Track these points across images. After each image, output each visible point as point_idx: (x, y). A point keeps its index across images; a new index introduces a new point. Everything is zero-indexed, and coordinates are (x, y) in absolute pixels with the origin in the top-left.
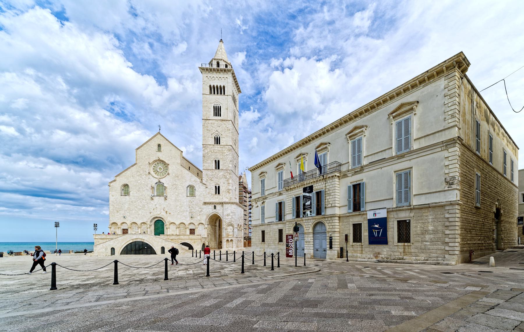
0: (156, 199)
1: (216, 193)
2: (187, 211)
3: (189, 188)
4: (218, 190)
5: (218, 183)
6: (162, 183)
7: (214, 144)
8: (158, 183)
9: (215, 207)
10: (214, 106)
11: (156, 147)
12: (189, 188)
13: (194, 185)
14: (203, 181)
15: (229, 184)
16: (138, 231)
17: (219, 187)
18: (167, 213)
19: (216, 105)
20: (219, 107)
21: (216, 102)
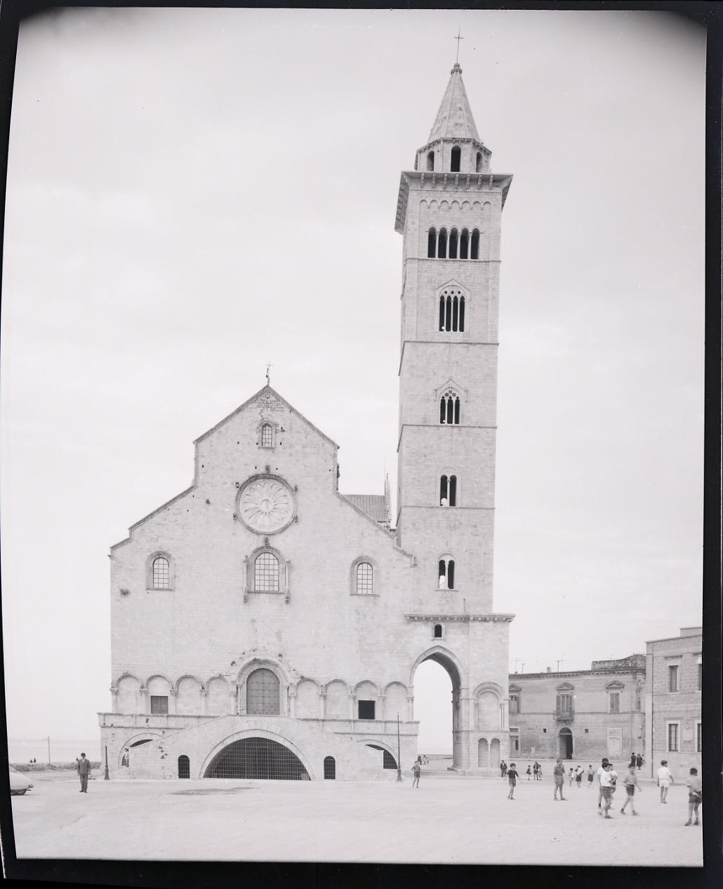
7: (439, 423)
9: (438, 632)
10: (442, 298)
12: (356, 566)
14: (402, 544)
19: (449, 293)
20: (459, 300)
21: (450, 284)
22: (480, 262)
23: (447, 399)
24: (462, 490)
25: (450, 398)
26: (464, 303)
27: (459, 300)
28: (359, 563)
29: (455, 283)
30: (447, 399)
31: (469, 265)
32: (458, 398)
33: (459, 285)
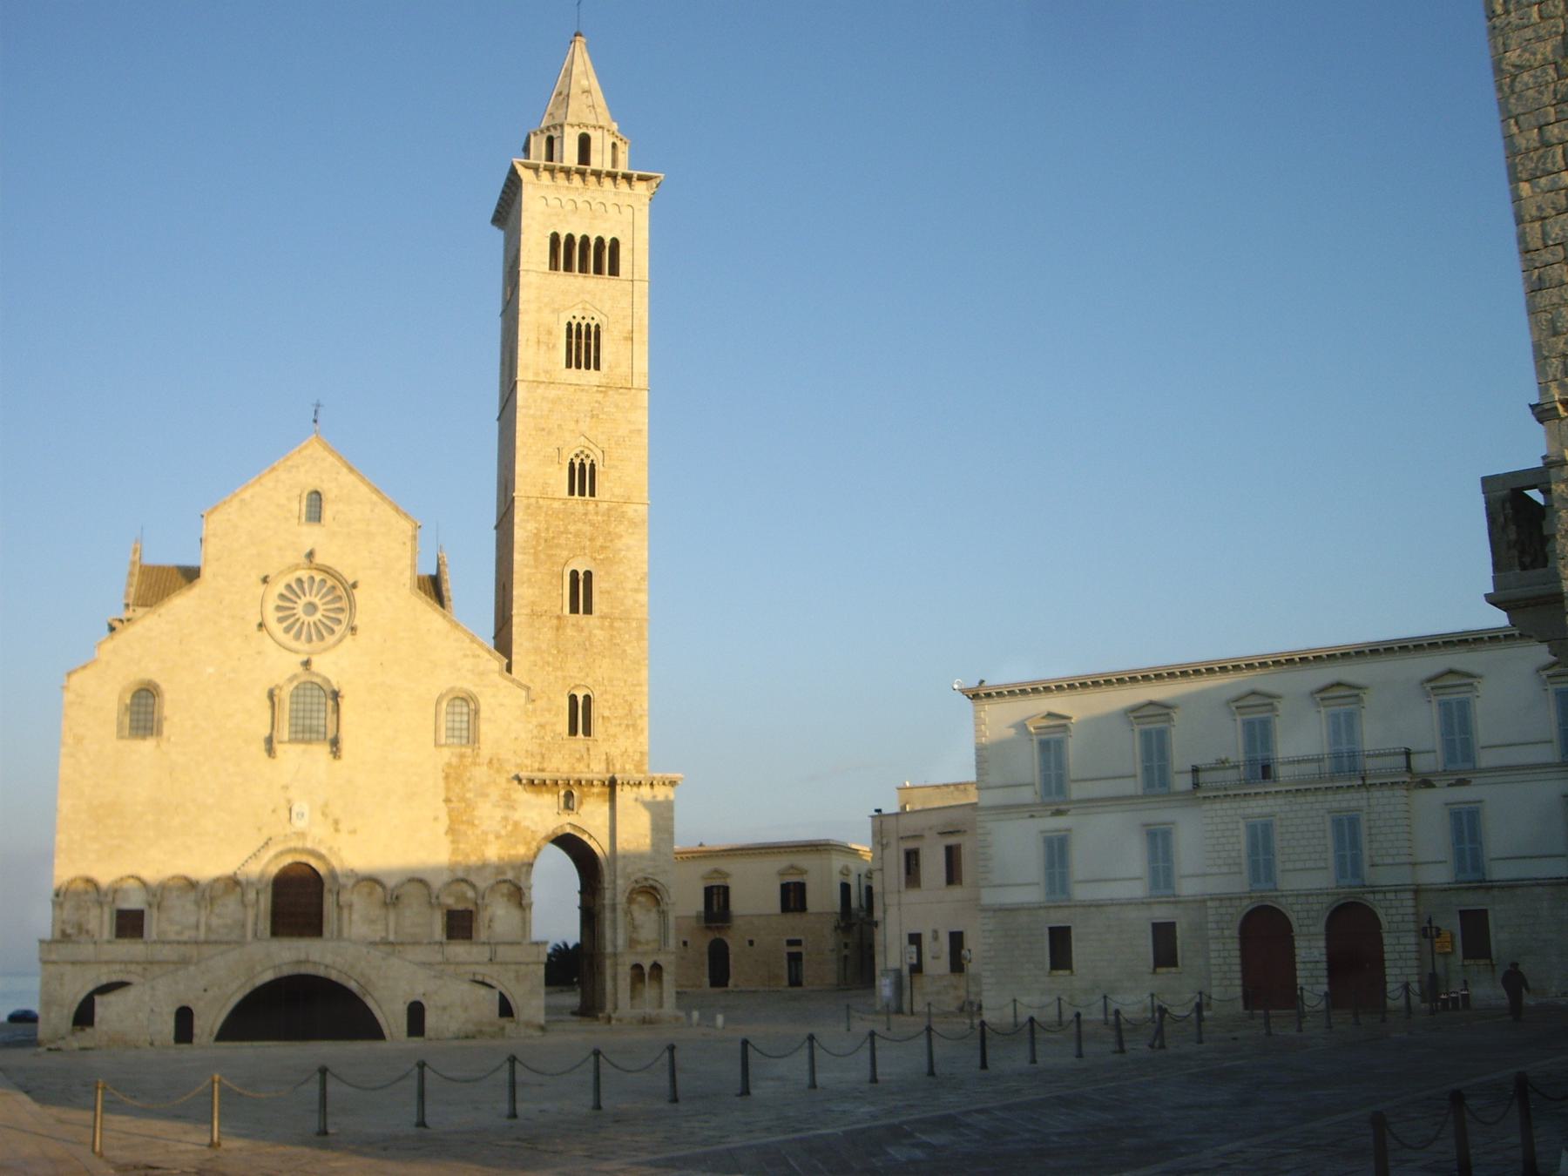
0: (289, 754)
1: (573, 730)
2: (436, 819)
3: (444, 705)
4: (580, 716)
5: (589, 681)
6: (318, 675)
8: (302, 679)
10: (569, 325)
11: (299, 507)
12: (444, 705)
13: (474, 690)
15: (638, 689)
16: (192, 920)
17: (587, 698)
18: (337, 830)
19: (579, 319)
20: (593, 329)
22: (621, 280)
23: (577, 463)
24: (601, 592)
25: (582, 460)
26: (599, 332)
27: (593, 329)
28: (451, 696)
29: (588, 306)
30: (577, 463)
31: (604, 283)
32: (592, 461)
33: (593, 309)
